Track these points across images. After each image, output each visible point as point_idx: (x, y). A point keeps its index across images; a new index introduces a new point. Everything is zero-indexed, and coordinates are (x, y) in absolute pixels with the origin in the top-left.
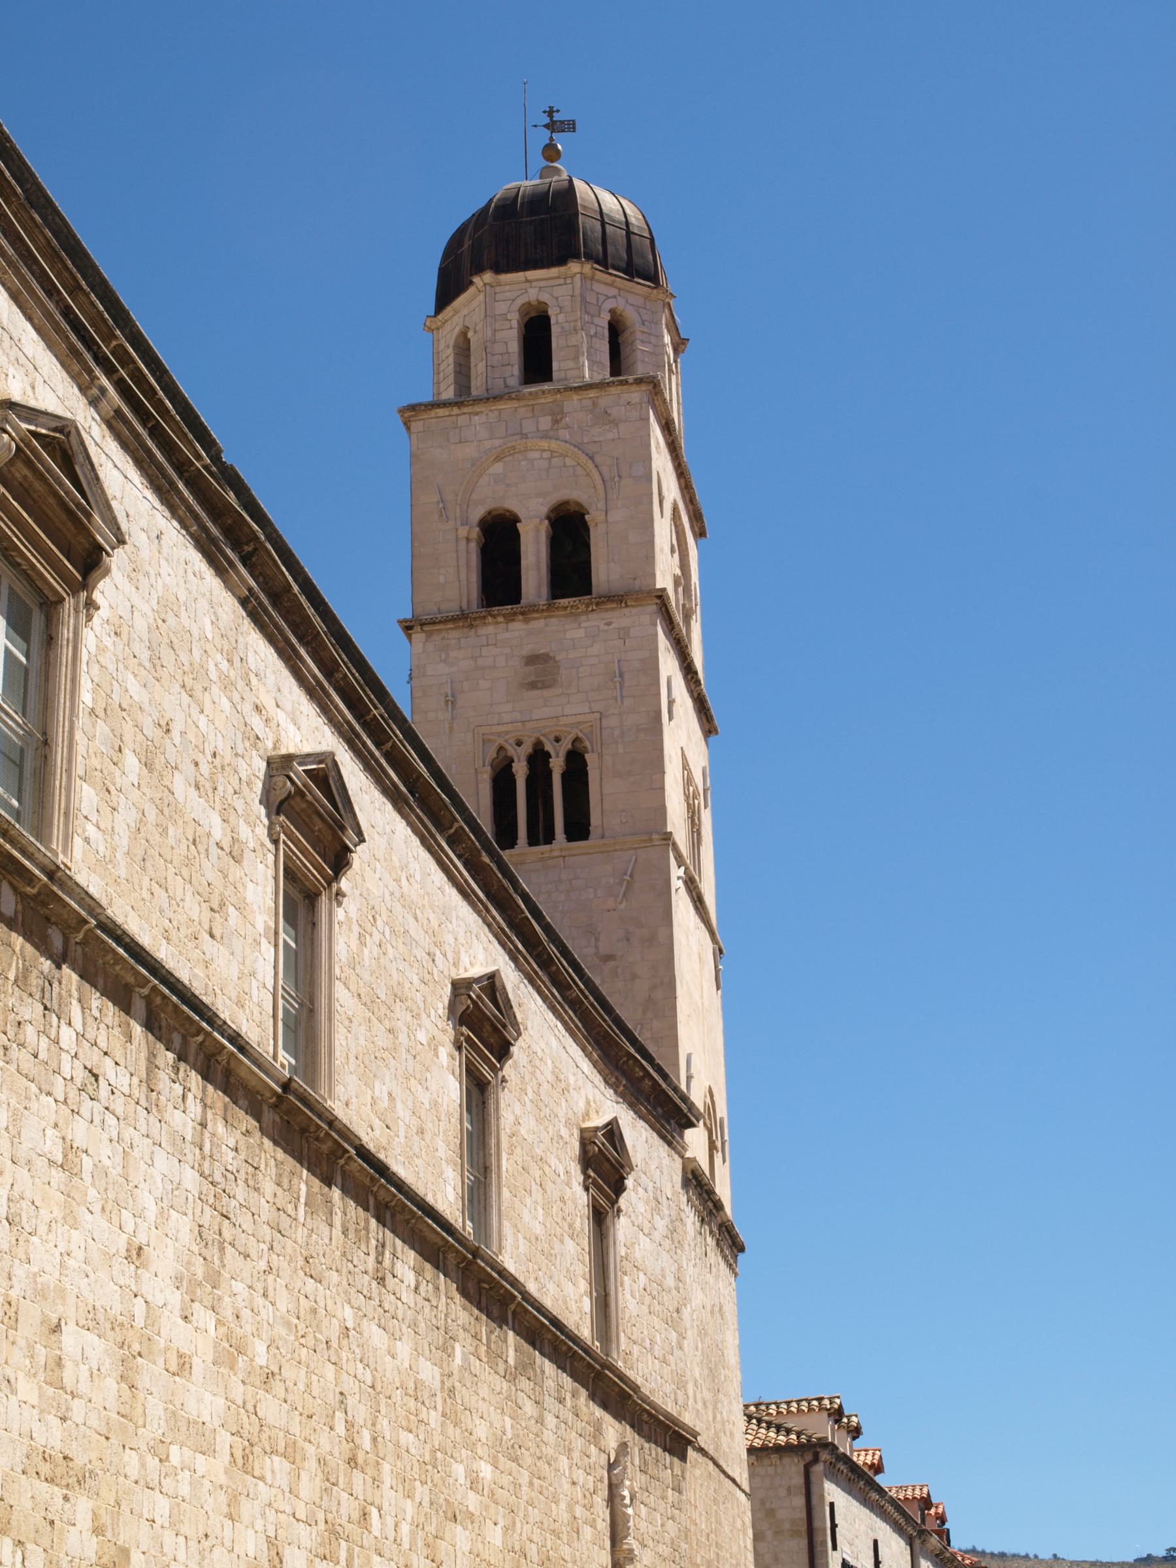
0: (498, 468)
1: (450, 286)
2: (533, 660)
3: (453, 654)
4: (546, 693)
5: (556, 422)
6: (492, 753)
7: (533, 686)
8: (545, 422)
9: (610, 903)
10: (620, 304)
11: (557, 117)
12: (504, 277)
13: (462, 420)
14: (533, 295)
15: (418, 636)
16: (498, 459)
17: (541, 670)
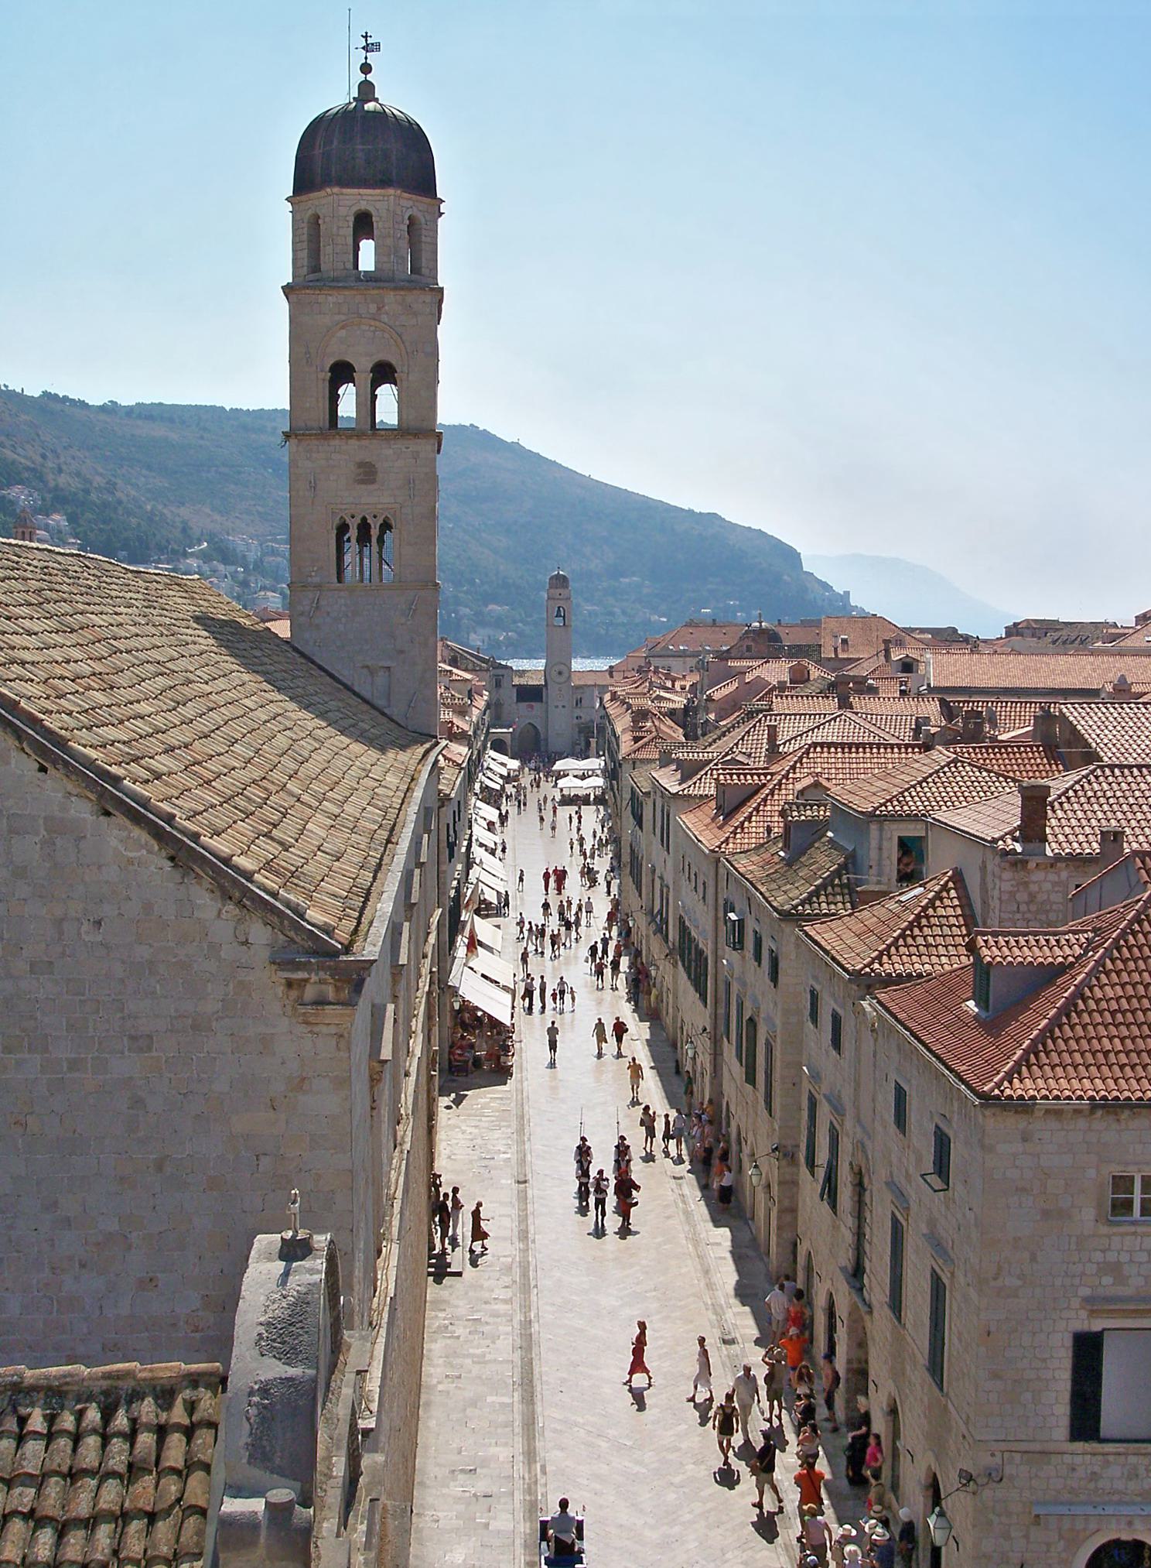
0: (343, 333)
1: (305, 181)
2: (360, 465)
3: (314, 455)
4: (371, 487)
5: (379, 309)
6: (337, 521)
7: (362, 482)
8: (373, 308)
9: (403, 620)
10: (415, 212)
11: (370, 41)
12: (345, 191)
13: (321, 299)
14: (363, 206)
15: (293, 441)
16: (343, 328)
17: (367, 473)
